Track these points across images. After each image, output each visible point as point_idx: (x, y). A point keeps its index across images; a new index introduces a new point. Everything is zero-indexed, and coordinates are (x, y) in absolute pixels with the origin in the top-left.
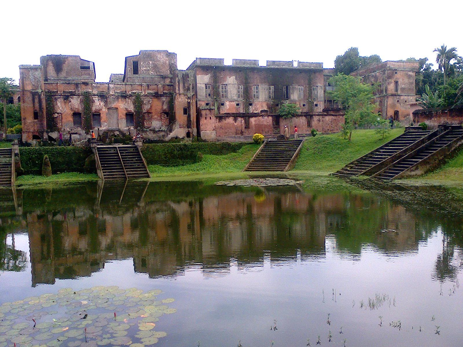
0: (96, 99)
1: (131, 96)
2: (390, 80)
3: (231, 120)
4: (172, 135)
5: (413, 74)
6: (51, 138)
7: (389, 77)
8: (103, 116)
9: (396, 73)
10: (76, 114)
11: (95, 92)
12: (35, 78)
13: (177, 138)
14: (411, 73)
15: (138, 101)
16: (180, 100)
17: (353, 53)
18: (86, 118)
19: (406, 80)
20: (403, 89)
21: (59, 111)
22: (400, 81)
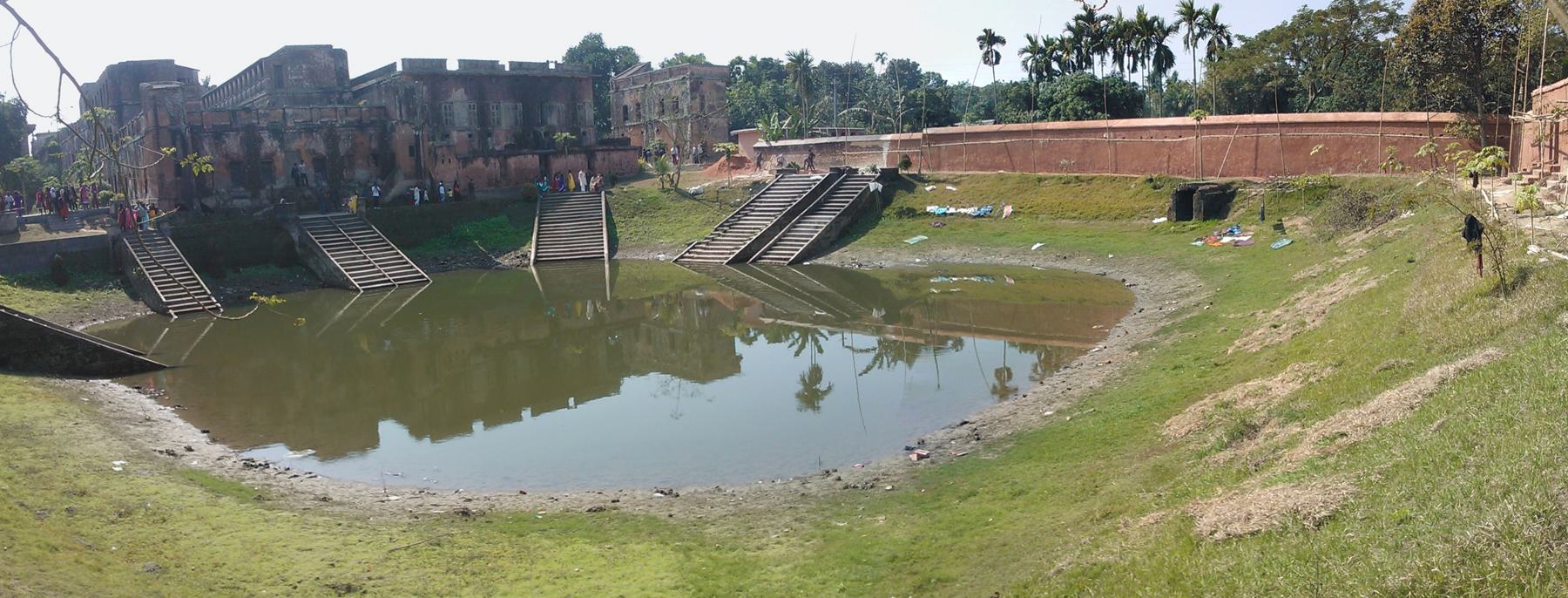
1: (320, 127)
4: (394, 192)
6: (205, 208)
11: (263, 124)
18: (250, 169)
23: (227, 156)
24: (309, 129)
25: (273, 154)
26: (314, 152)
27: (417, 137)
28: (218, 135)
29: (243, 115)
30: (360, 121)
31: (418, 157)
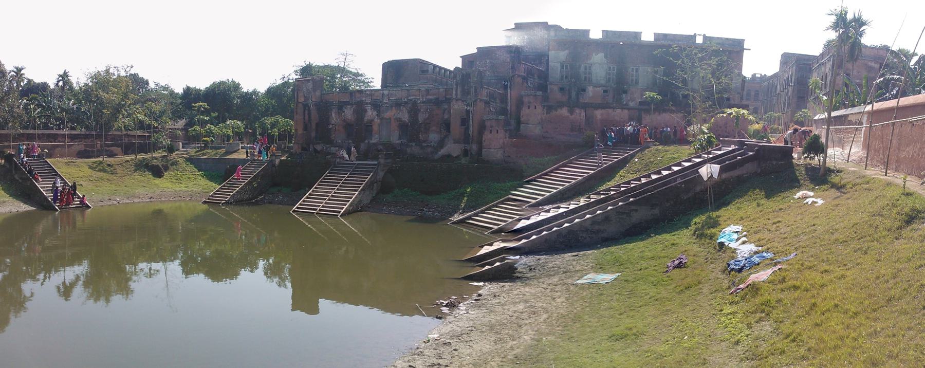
0: (369, 107)
1: (406, 103)
4: (443, 152)
6: (316, 151)
8: (375, 128)
10: (348, 126)
11: (368, 100)
12: (308, 90)
13: (449, 156)
15: (414, 110)
16: (456, 107)
17: (188, 88)
21: (333, 122)
23: (344, 121)
24: (398, 104)
25: (372, 121)
26: (399, 120)
27: (468, 112)
28: (341, 107)
29: (358, 95)
30: (437, 99)
31: (468, 128)
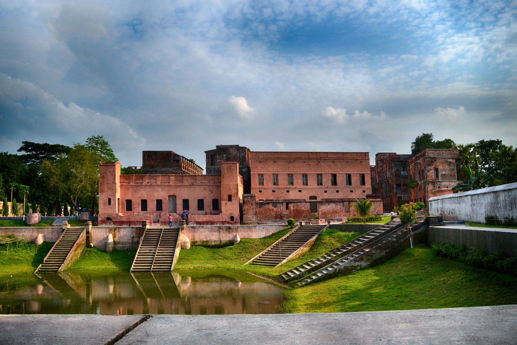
2: (430, 167)
3: (271, 206)
5: (454, 161)
7: (430, 165)
9: (435, 160)
14: (451, 160)
19: (447, 167)
20: (443, 176)
22: (440, 167)
